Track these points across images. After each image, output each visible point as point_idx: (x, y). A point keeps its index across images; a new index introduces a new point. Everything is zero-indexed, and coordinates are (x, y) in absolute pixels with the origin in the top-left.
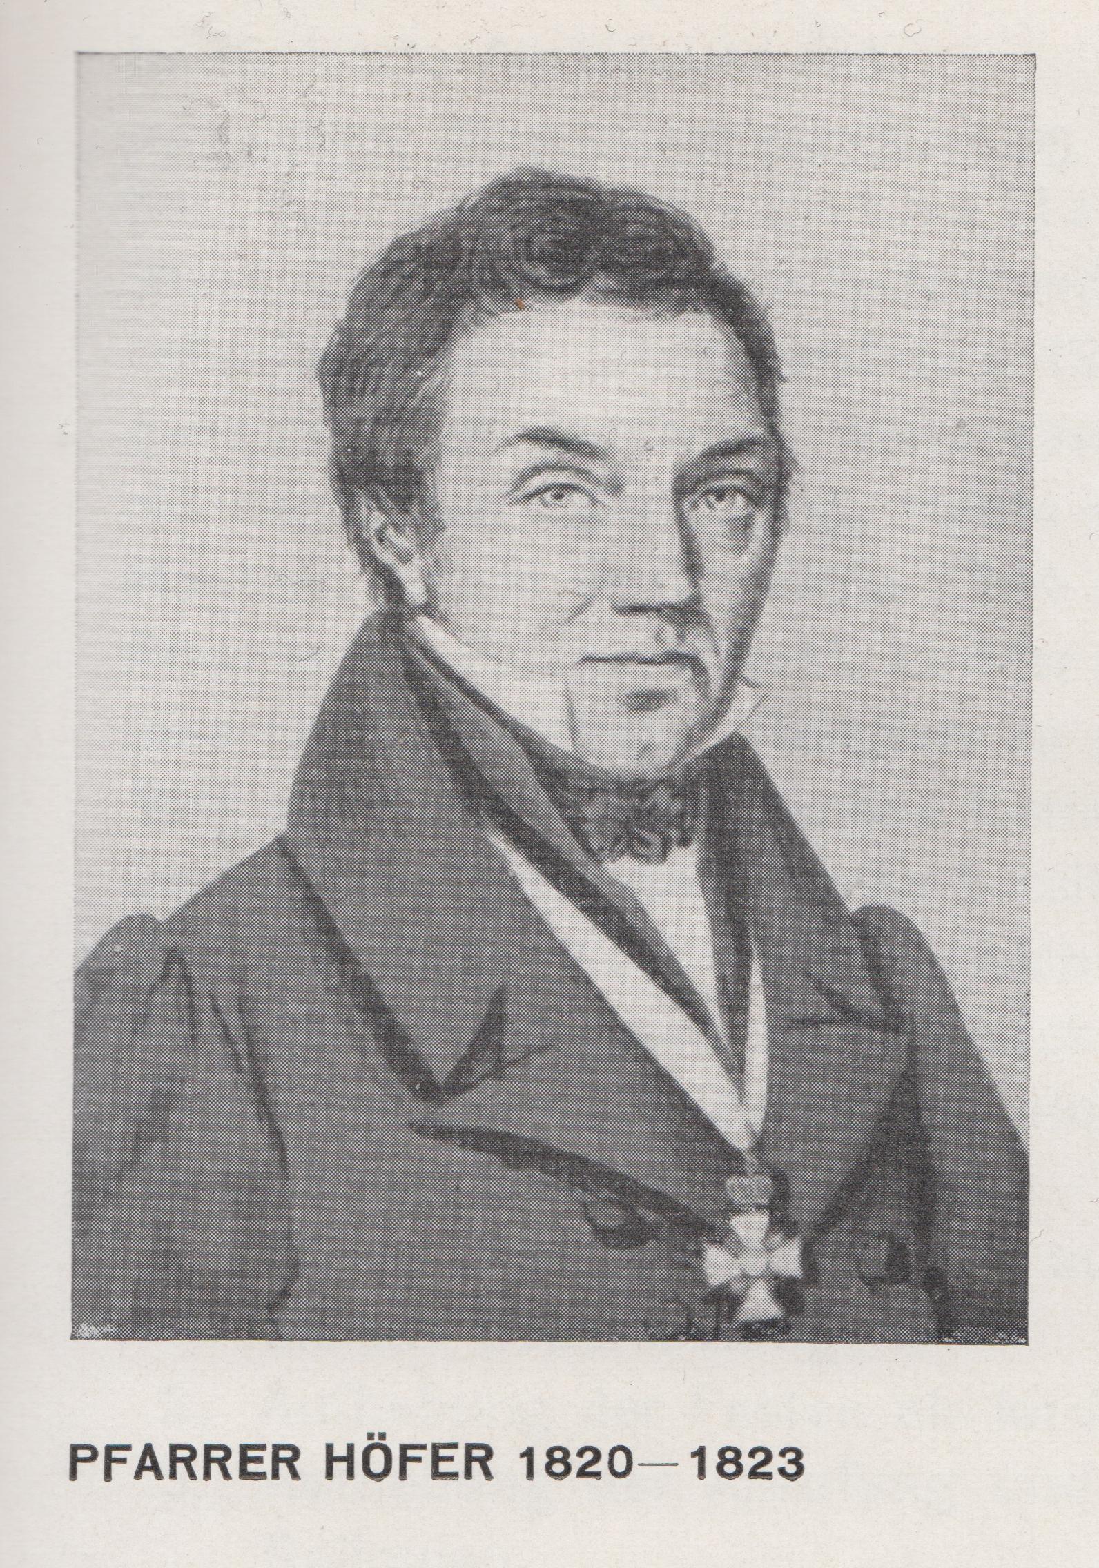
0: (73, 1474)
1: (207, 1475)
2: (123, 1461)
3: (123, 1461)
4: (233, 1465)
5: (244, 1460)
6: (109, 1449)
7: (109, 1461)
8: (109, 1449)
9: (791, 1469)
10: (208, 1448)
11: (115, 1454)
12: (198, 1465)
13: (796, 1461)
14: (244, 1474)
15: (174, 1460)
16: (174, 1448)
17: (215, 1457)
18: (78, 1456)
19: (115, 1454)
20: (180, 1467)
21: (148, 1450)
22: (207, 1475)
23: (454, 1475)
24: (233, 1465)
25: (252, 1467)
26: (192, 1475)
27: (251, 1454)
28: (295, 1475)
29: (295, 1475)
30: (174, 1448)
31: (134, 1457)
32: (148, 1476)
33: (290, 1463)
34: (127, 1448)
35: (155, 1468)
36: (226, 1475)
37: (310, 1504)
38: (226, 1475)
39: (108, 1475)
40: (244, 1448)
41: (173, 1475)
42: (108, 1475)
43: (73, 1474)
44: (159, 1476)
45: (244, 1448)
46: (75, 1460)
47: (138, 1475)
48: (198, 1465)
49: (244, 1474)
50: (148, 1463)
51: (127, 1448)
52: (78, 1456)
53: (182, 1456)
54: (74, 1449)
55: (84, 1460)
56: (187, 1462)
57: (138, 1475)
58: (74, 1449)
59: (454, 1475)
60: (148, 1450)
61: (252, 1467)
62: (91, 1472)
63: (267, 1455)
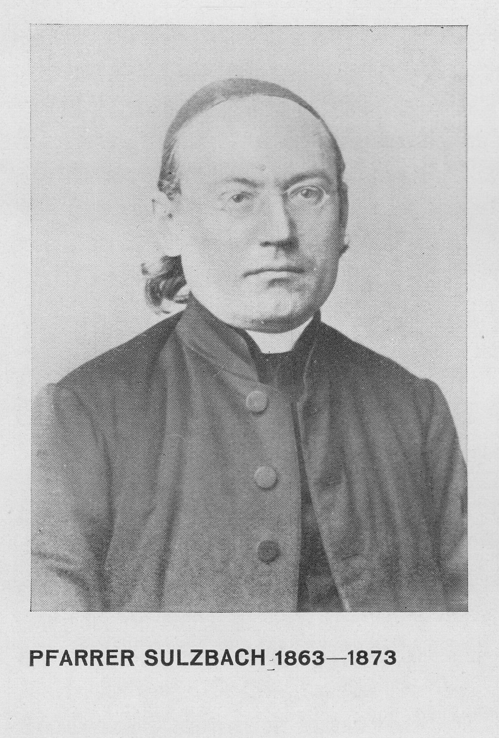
0: (32, 664)
1: (92, 664)
2: (55, 657)
3: (55, 657)
4: (104, 659)
5: (109, 657)
6: (48, 652)
7: (48, 657)
8: (48, 652)
9: (390, 660)
10: (92, 652)
11: (51, 654)
12: (88, 659)
13: (321, 657)
14: (109, 663)
15: (77, 657)
16: (77, 652)
17: (96, 656)
18: (34, 656)
19: (51, 654)
20: (80, 660)
21: (66, 653)
22: (92, 664)
23: (116, 664)
24: (104, 659)
25: (112, 660)
26: (86, 664)
27: (111, 654)
28: (132, 664)
29: (132, 664)
30: (77, 652)
31: (60, 656)
32: (66, 664)
33: (130, 658)
34: (57, 651)
35: (69, 661)
36: (101, 664)
37: (338, 672)
38: (101, 664)
39: (48, 664)
40: (108, 652)
41: (77, 664)
42: (48, 664)
43: (32, 664)
44: (71, 664)
45: (108, 652)
46: (32, 658)
47: (61, 664)
48: (88, 659)
49: (109, 663)
50: (66, 659)
51: (57, 651)
52: (34, 656)
53: (81, 655)
54: (32, 652)
55: (36, 657)
56: (83, 658)
57: (61, 664)
58: (32, 652)
59: (116, 664)
60: (66, 653)
61: (112, 660)
62: (40, 663)
63: (119, 654)
